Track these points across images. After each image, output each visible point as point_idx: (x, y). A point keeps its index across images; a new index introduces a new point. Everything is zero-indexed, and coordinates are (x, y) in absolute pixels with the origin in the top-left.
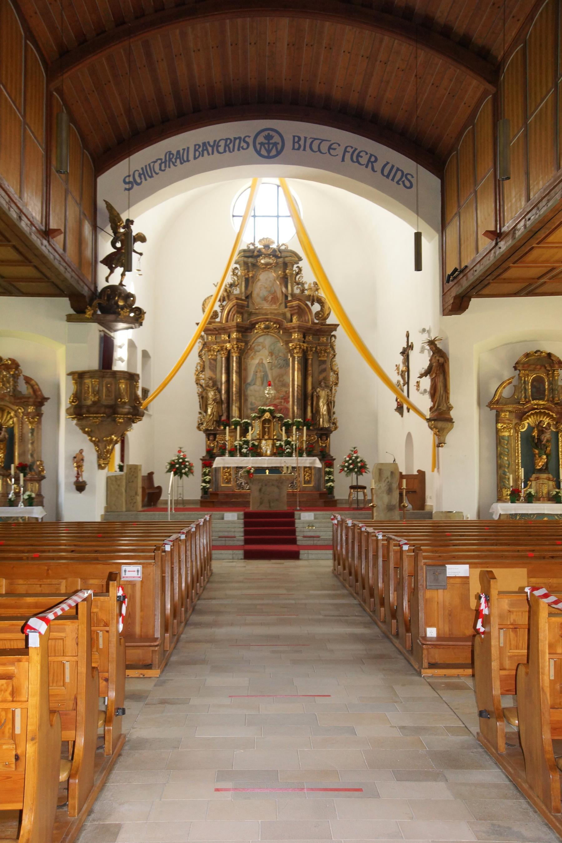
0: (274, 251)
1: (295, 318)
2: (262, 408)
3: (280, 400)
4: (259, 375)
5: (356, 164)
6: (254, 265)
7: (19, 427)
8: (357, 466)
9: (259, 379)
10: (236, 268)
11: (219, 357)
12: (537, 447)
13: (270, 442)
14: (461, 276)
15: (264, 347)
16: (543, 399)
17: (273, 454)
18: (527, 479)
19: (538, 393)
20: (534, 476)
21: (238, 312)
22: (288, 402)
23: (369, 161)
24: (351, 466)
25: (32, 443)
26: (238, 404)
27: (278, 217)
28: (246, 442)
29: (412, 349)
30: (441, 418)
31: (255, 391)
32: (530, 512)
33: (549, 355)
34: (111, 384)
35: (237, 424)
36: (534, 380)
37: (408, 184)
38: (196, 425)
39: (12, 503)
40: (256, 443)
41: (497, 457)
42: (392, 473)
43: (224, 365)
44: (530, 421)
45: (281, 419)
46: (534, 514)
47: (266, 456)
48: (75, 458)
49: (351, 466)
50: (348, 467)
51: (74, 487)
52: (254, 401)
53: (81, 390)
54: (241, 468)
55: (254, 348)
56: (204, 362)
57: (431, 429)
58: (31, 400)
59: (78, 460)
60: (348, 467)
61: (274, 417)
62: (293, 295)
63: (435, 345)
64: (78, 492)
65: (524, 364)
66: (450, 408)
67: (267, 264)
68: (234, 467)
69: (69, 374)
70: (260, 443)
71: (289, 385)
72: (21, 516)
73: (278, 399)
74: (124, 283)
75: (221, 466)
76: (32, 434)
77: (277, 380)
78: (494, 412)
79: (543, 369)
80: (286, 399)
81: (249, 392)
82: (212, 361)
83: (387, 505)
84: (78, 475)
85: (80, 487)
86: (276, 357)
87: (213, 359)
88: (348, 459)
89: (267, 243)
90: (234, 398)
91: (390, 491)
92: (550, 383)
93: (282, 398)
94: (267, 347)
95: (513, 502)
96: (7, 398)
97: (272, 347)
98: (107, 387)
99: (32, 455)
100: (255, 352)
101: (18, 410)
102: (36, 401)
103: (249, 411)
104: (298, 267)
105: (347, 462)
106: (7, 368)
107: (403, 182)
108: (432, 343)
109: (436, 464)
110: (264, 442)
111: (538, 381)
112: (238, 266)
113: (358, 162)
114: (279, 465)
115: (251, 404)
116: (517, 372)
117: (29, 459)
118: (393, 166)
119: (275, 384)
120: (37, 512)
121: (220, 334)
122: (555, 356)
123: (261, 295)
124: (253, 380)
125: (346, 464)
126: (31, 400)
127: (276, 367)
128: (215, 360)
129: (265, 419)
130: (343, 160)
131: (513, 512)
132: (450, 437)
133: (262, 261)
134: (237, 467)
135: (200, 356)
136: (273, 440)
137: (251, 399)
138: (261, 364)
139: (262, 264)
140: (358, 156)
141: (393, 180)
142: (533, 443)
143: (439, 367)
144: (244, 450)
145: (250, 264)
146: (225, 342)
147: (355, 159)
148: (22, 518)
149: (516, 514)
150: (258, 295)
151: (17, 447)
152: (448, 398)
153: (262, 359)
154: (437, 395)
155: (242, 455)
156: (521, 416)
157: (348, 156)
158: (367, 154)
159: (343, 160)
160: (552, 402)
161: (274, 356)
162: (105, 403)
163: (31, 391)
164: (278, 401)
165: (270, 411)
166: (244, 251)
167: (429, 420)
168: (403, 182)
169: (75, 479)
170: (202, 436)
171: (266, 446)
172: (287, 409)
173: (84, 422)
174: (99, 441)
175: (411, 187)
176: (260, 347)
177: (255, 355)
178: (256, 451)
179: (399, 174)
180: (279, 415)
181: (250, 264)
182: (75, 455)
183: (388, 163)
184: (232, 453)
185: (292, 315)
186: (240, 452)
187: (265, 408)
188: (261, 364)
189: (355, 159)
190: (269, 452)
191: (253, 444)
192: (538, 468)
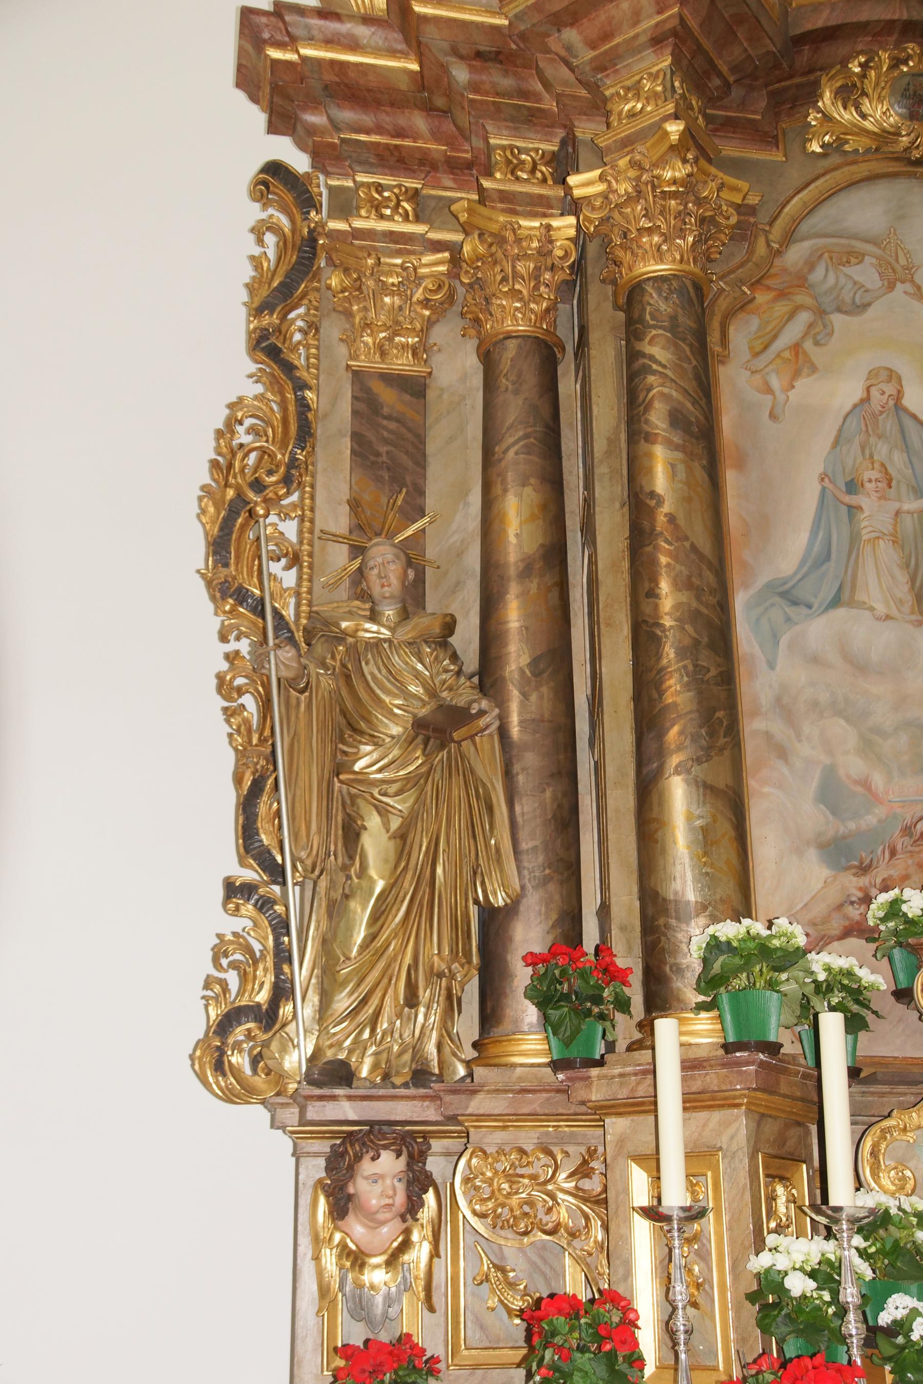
4: (874, 513)
9: (887, 552)
31: (859, 666)
38: (194, 1021)
52: (853, 766)
55: (801, 281)
82: (388, 396)
87: (388, 378)
100: (821, 313)
124: (819, 558)
153: (892, 376)
170: (257, 1162)
176: (866, 274)
177: (820, 330)
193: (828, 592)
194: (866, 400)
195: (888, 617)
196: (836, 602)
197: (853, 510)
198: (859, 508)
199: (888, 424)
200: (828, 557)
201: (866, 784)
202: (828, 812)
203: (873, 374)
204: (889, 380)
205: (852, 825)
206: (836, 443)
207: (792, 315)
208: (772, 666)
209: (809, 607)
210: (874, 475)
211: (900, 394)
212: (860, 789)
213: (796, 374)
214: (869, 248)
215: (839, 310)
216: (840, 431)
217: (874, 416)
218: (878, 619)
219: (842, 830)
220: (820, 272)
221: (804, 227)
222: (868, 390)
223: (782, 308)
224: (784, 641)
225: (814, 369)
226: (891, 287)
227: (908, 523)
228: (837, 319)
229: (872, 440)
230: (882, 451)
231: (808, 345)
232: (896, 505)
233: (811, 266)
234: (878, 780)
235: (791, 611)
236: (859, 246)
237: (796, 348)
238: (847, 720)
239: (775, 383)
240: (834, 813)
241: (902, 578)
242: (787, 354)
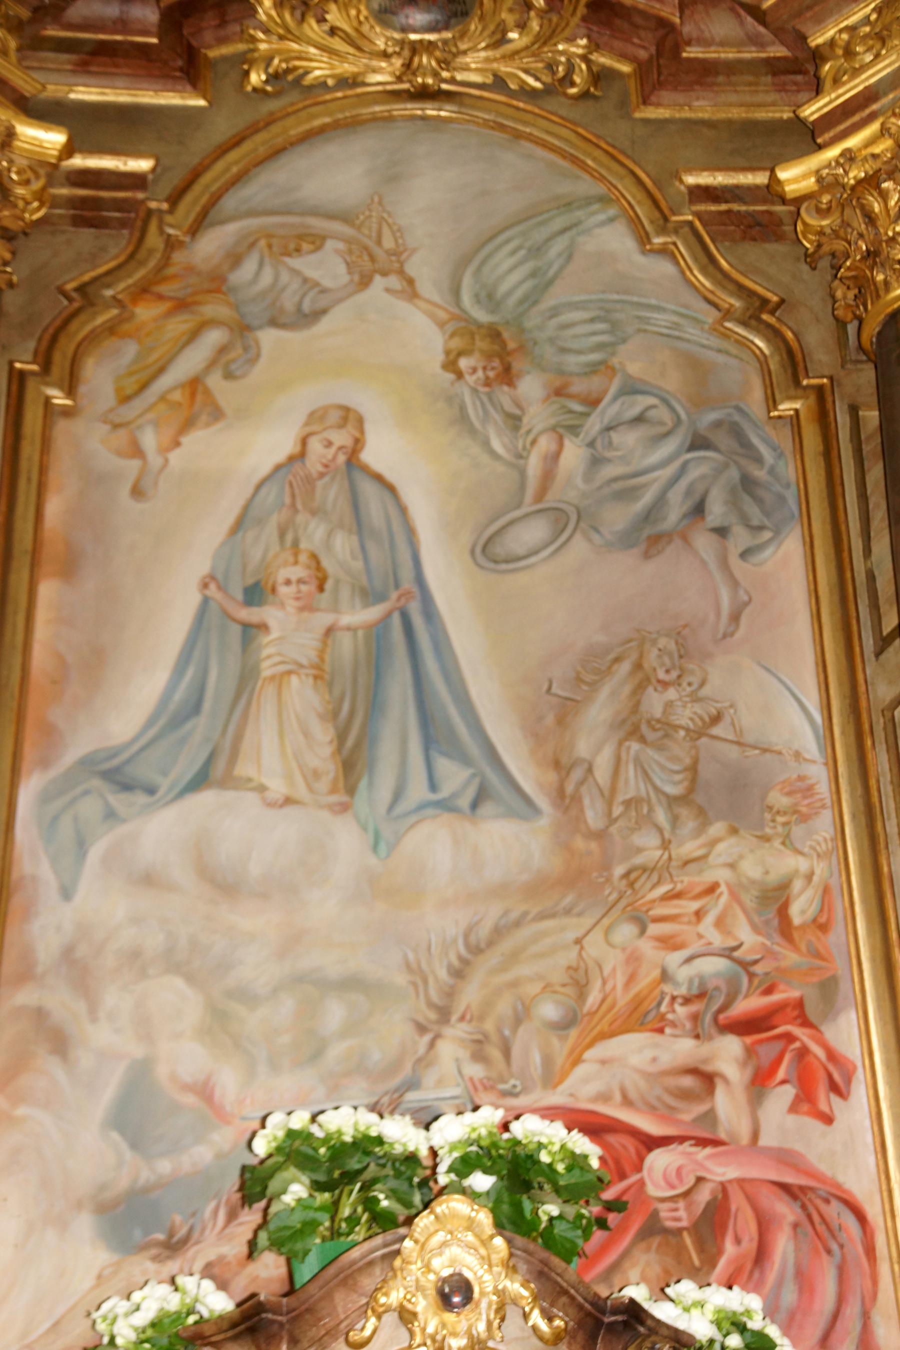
2: (345, 1121)
3: (681, 1048)
4: (288, 632)
9: (302, 695)
15: (376, 261)
31: (224, 884)
52: (185, 1057)
55: (216, 283)
73: (644, 1017)
77: (600, 712)
86: (574, 402)
93: (714, 1013)
94: (426, 269)
97: (509, 274)
100: (242, 329)
119: (560, 765)
124: (178, 714)
127: (565, 522)
138: (334, 474)
153: (349, 417)
161: (531, 386)
164: (637, 1055)
176: (327, 267)
187: (401, 1134)
193: (187, 765)
194: (299, 456)
195: (288, 801)
196: (200, 781)
197: (251, 631)
198: (263, 627)
199: (332, 493)
200: (196, 708)
201: (205, 1091)
202: (124, 1146)
203: (316, 417)
204: (342, 424)
205: (165, 1166)
206: (238, 526)
207: (194, 335)
208: (67, 894)
209: (151, 791)
210: (296, 572)
211: (358, 443)
212: (190, 1099)
213: (188, 425)
214: (337, 227)
215: (274, 323)
216: (246, 508)
217: (310, 481)
218: (271, 805)
219: (145, 1176)
220: (249, 266)
221: (229, 203)
222: (304, 442)
223: (178, 325)
224: (95, 853)
225: (217, 414)
226: (365, 282)
227: (346, 645)
228: (268, 337)
229: (301, 518)
230: (314, 534)
231: (215, 381)
232: (324, 619)
233: (235, 259)
234: (228, 1082)
235: (118, 801)
236: (318, 224)
237: (194, 385)
238: (190, 979)
239: (149, 440)
240: (134, 1146)
241: (324, 734)
242: (177, 396)
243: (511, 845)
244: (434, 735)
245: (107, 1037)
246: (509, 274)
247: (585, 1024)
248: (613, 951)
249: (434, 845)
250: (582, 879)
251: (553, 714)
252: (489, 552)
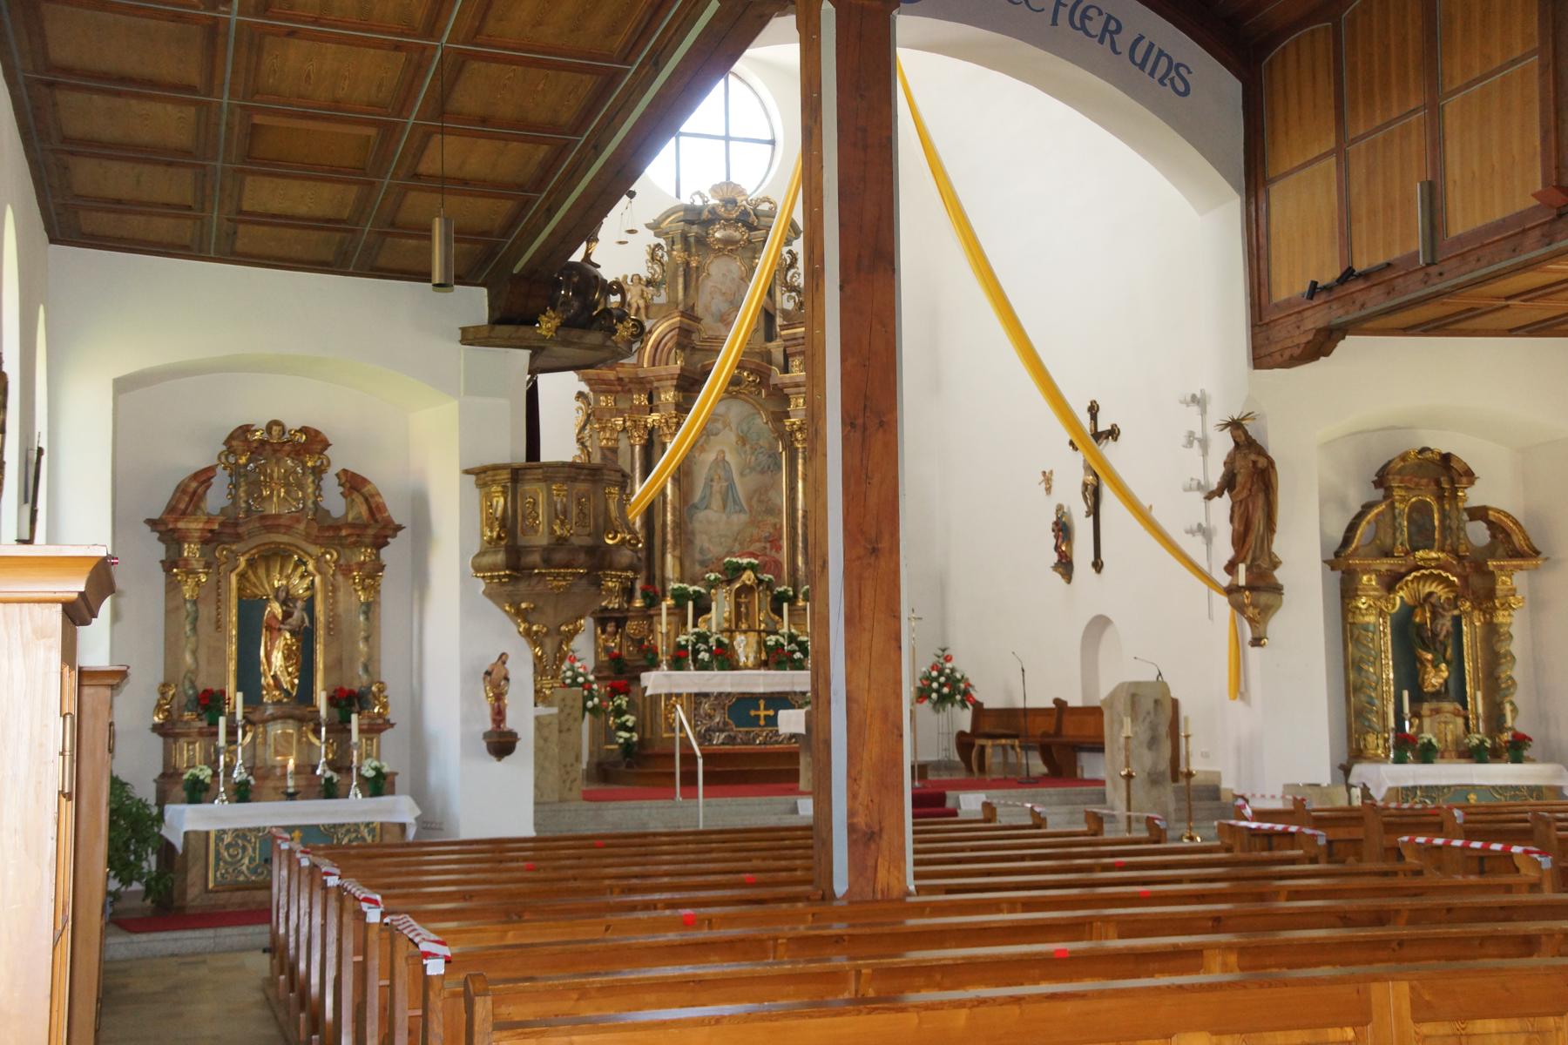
0: (745, 213)
1: (796, 362)
4: (716, 487)
5: (1081, 33)
6: (701, 241)
7: (326, 598)
8: (945, 688)
9: (718, 497)
10: (659, 246)
11: (623, 444)
12: (1427, 649)
13: (753, 637)
14: (1361, 285)
15: (726, 425)
16: (1431, 548)
17: (763, 664)
18: (1416, 714)
19: (1422, 536)
20: (1426, 708)
21: (680, 346)
22: (779, 548)
23: (1105, 29)
24: (946, 690)
25: (367, 639)
26: (677, 553)
27: (727, 138)
28: (702, 638)
29: (1115, 439)
30: (1254, 588)
31: (709, 522)
32: (1444, 782)
33: (1446, 458)
34: (588, 499)
35: (681, 597)
36: (1413, 508)
37: (1181, 88)
39: (330, 791)
40: (726, 641)
41: (1346, 667)
42: (1156, 702)
43: (637, 465)
44: (1401, 596)
45: (769, 586)
46: (1449, 787)
47: (746, 668)
48: (488, 673)
49: (946, 690)
50: (938, 691)
51: (484, 745)
52: (706, 545)
53: (515, 511)
54: (706, 695)
56: (589, 454)
57: (1239, 607)
58: (371, 532)
59: (496, 680)
60: (938, 691)
61: (761, 582)
62: (785, 313)
63: (1246, 433)
64: (493, 759)
65: (1400, 472)
66: (1275, 564)
67: (727, 241)
68: (689, 695)
69: (467, 472)
70: (732, 639)
71: (780, 511)
72: (368, 820)
73: (759, 540)
74: (593, 259)
75: (663, 690)
76: (366, 613)
78: (1338, 574)
79: (1433, 487)
80: (775, 542)
81: (697, 526)
83: (1149, 774)
84: (499, 714)
85: (502, 744)
86: (754, 450)
87: (609, 449)
88: (935, 674)
89: (729, 195)
90: (670, 537)
91: (1153, 742)
92: (1444, 516)
93: (767, 540)
94: (733, 426)
95: (1400, 760)
96: (302, 526)
97: (745, 428)
98: (579, 503)
99: (366, 668)
101: (323, 555)
102: (368, 530)
103: (698, 568)
104: (790, 252)
105: (936, 679)
106: (299, 451)
107: (1172, 80)
108: (1235, 425)
109: (1239, 687)
110: (740, 639)
111: (1421, 509)
112: (662, 242)
113: (1083, 28)
114: (788, 689)
115: (702, 551)
116: (1381, 492)
117: (357, 680)
118: (1151, 45)
119: (751, 506)
120: (400, 809)
121: (630, 391)
122: (1459, 460)
123: (714, 308)
124: (703, 498)
125: (935, 685)
126: (371, 532)
128: (614, 451)
129: (744, 586)
130: (1054, 23)
131: (1410, 783)
132: (1276, 626)
133: (717, 235)
134: (697, 695)
135: (580, 441)
136: (759, 632)
137: (701, 541)
138: (721, 462)
139: (719, 240)
140: (1084, 16)
141: (1152, 74)
142: (1411, 637)
143: (1250, 479)
144: (704, 656)
145: (692, 240)
146: (639, 409)
147: (1078, 23)
148: (367, 825)
149: (1415, 788)
150: (707, 309)
151: (319, 648)
152: (1270, 542)
154: (1252, 539)
155: (702, 666)
156: (1391, 582)
157: (1064, 13)
158: (1100, 13)
159: (1054, 23)
160: (1454, 552)
162: (576, 541)
163: (364, 510)
165: (751, 567)
166: (689, 209)
167: (1231, 591)
168: (1172, 80)
169: (489, 726)
171: (744, 647)
172: (778, 564)
173: (523, 587)
174: (546, 634)
175: (1186, 93)
176: (719, 425)
178: (724, 658)
179: (1164, 62)
180: (767, 577)
181: (692, 240)
182: (487, 667)
183: (1141, 38)
184: (677, 663)
185: (786, 357)
186: (695, 660)
188: (721, 462)
189: (1078, 23)
190: (751, 659)
191: (718, 641)
192: (1430, 689)
243: (744, 517)
244: (735, 502)
245: (698, 542)
246: (745, 428)
247: (752, 541)
248: (755, 531)
249: (735, 518)
250: (754, 522)
251: (749, 499)
252: (742, 474)
